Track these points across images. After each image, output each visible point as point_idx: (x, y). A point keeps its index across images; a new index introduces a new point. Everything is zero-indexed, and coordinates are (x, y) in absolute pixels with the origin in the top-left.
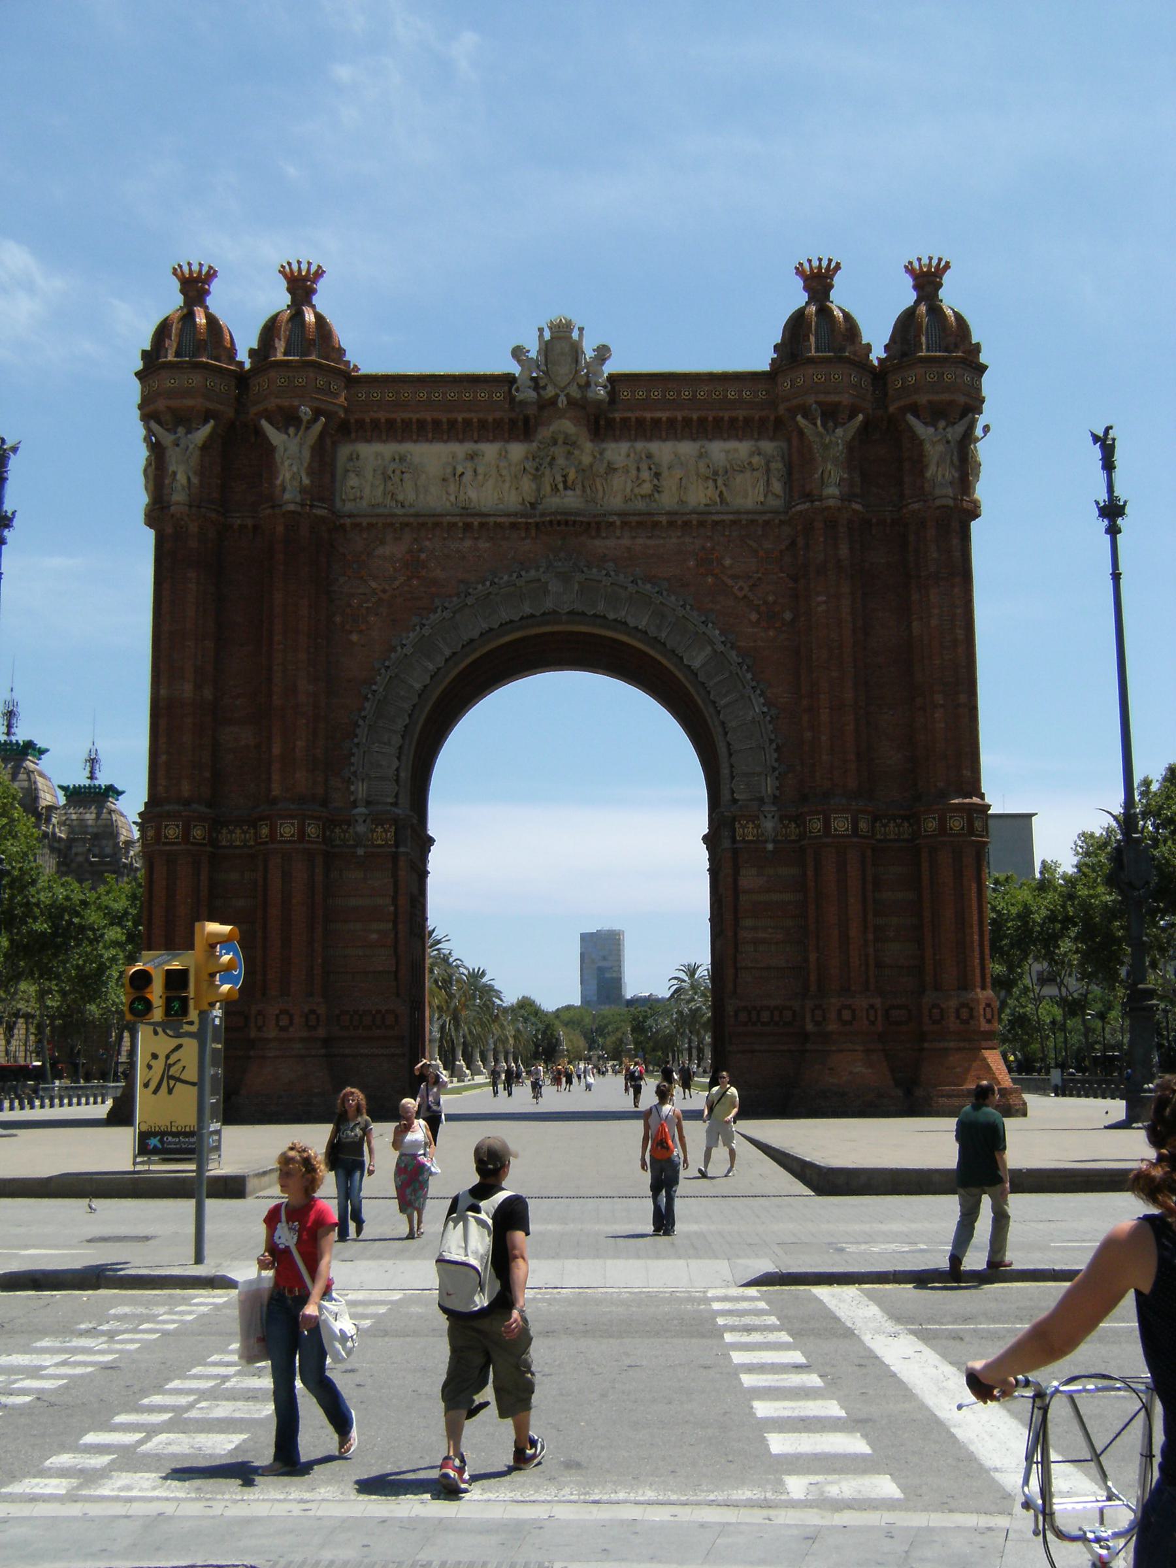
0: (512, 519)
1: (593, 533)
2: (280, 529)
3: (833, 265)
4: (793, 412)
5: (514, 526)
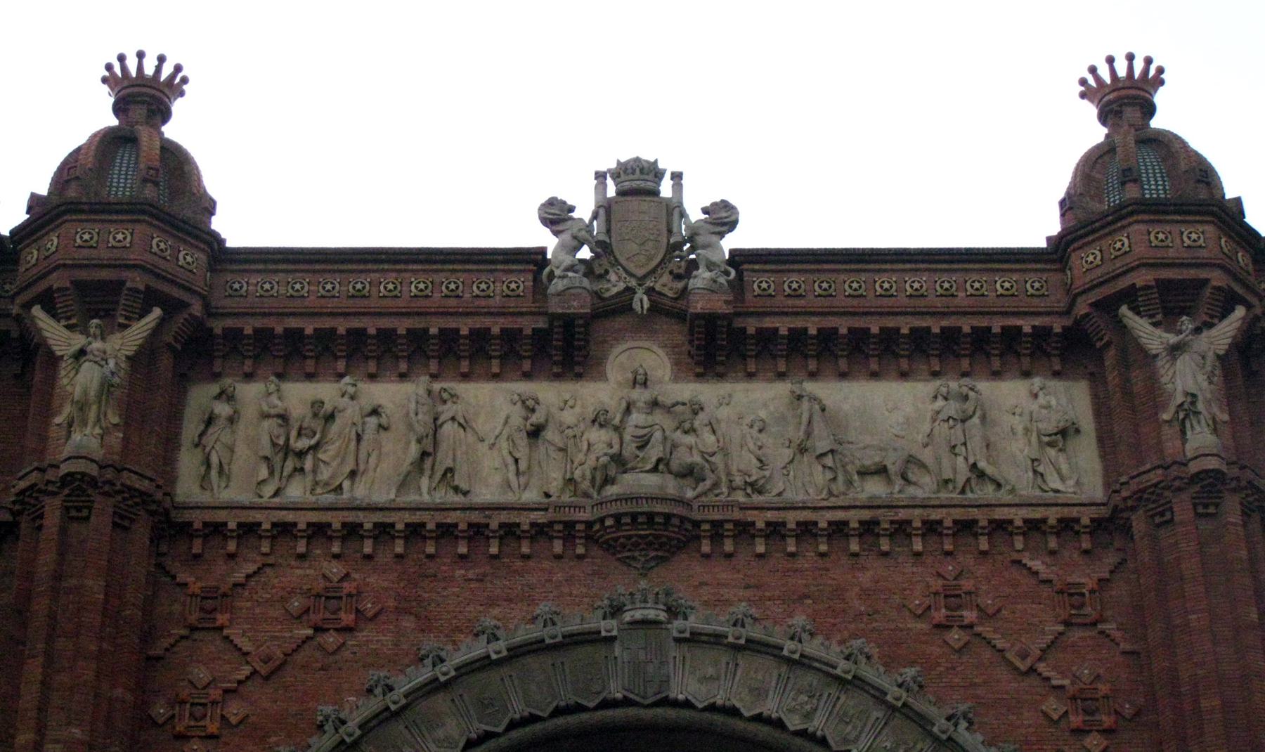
0: (539, 517)
1: (706, 548)
2: (52, 511)
3: (1152, 72)
4: (1108, 306)
5: (540, 532)
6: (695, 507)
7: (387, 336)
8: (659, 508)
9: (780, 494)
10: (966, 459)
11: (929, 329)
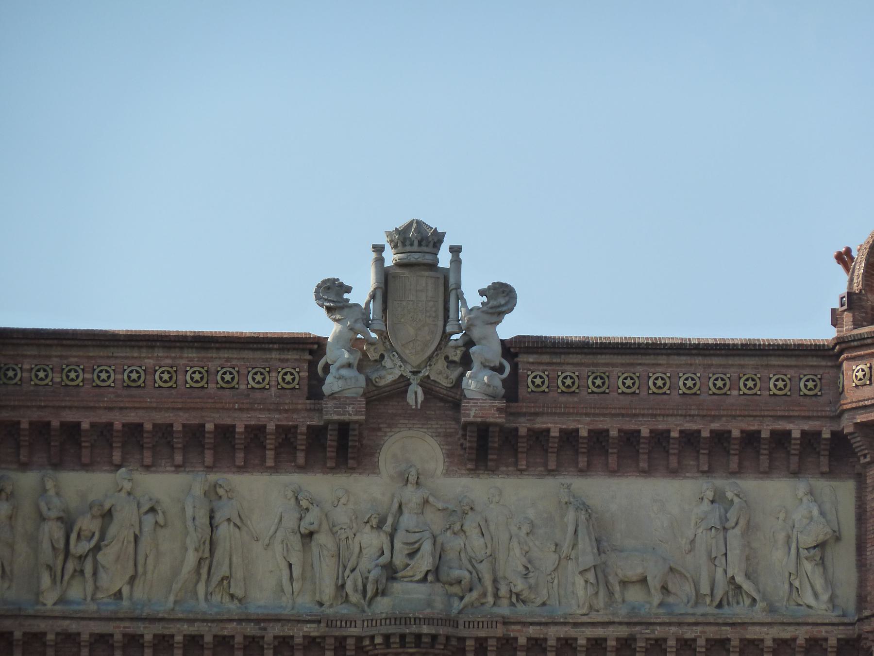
0: (311, 630)
6: (461, 622)
7: (165, 431)
8: (425, 629)
9: (544, 604)
10: (725, 571)
11: (699, 432)
